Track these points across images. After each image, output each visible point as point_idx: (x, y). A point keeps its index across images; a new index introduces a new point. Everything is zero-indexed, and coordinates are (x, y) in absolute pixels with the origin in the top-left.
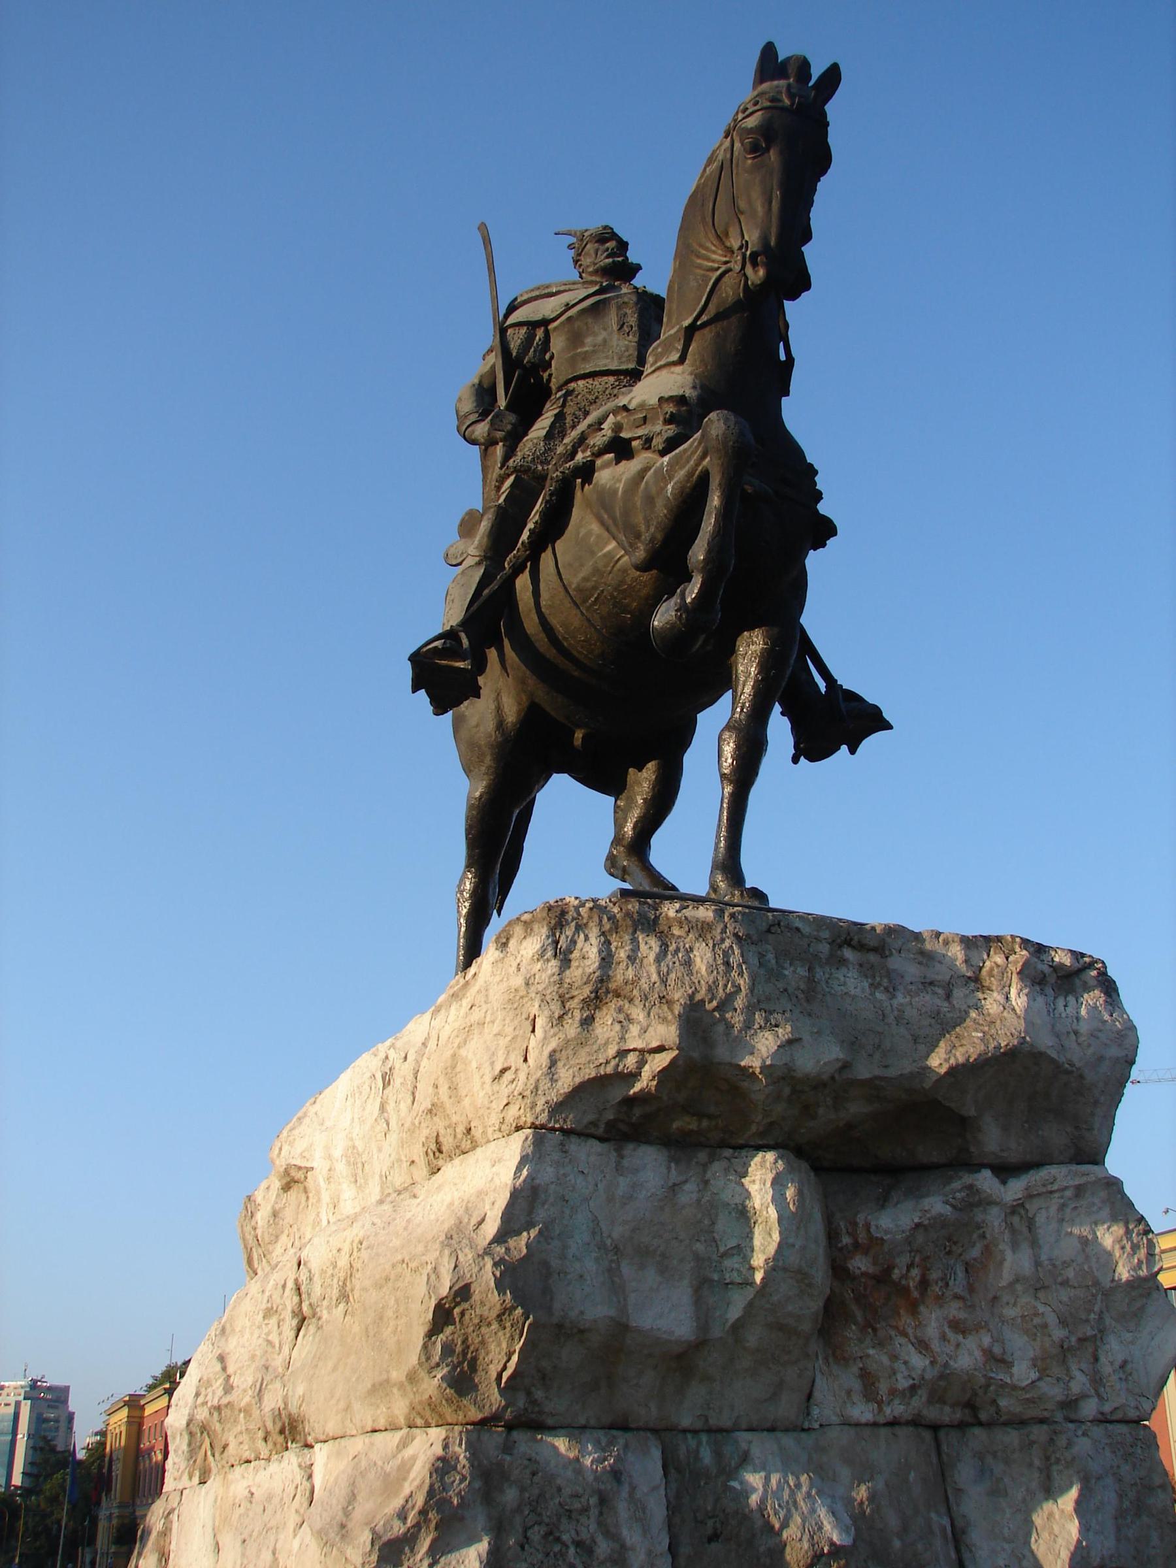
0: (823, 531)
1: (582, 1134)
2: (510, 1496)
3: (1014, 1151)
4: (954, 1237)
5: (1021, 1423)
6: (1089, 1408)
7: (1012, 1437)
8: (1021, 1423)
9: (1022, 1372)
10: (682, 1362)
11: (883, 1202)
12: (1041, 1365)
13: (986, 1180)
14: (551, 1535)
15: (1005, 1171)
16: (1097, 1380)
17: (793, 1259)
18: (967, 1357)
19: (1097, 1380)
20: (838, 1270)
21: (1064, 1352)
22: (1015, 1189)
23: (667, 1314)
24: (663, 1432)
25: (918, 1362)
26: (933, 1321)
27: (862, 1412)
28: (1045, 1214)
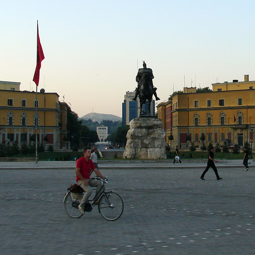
0: (156, 89)
1: (137, 128)
2: (134, 142)
3: (156, 128)
4: (154, 131)
5: (157, 139)
6: (160, 138)
7: (157, 139)
8: (157, 139)
9: (157, 137)
10: (141, 137)
11: (150, 130)
12: (158, 136)
13: (155, 129)
14: (136, 143)
15: (156, 128)
16: (160, 137)
17: (231, 102)
18: (154, 136)
19: (160, 137)
20: (148, 133)
21: (159, 136)
22: (156, 129)
23: (140, 135)
24: (141, 139)
25: (152, 136)
26: (153, 135)
27: (150, 138)
28: (158, 130)
